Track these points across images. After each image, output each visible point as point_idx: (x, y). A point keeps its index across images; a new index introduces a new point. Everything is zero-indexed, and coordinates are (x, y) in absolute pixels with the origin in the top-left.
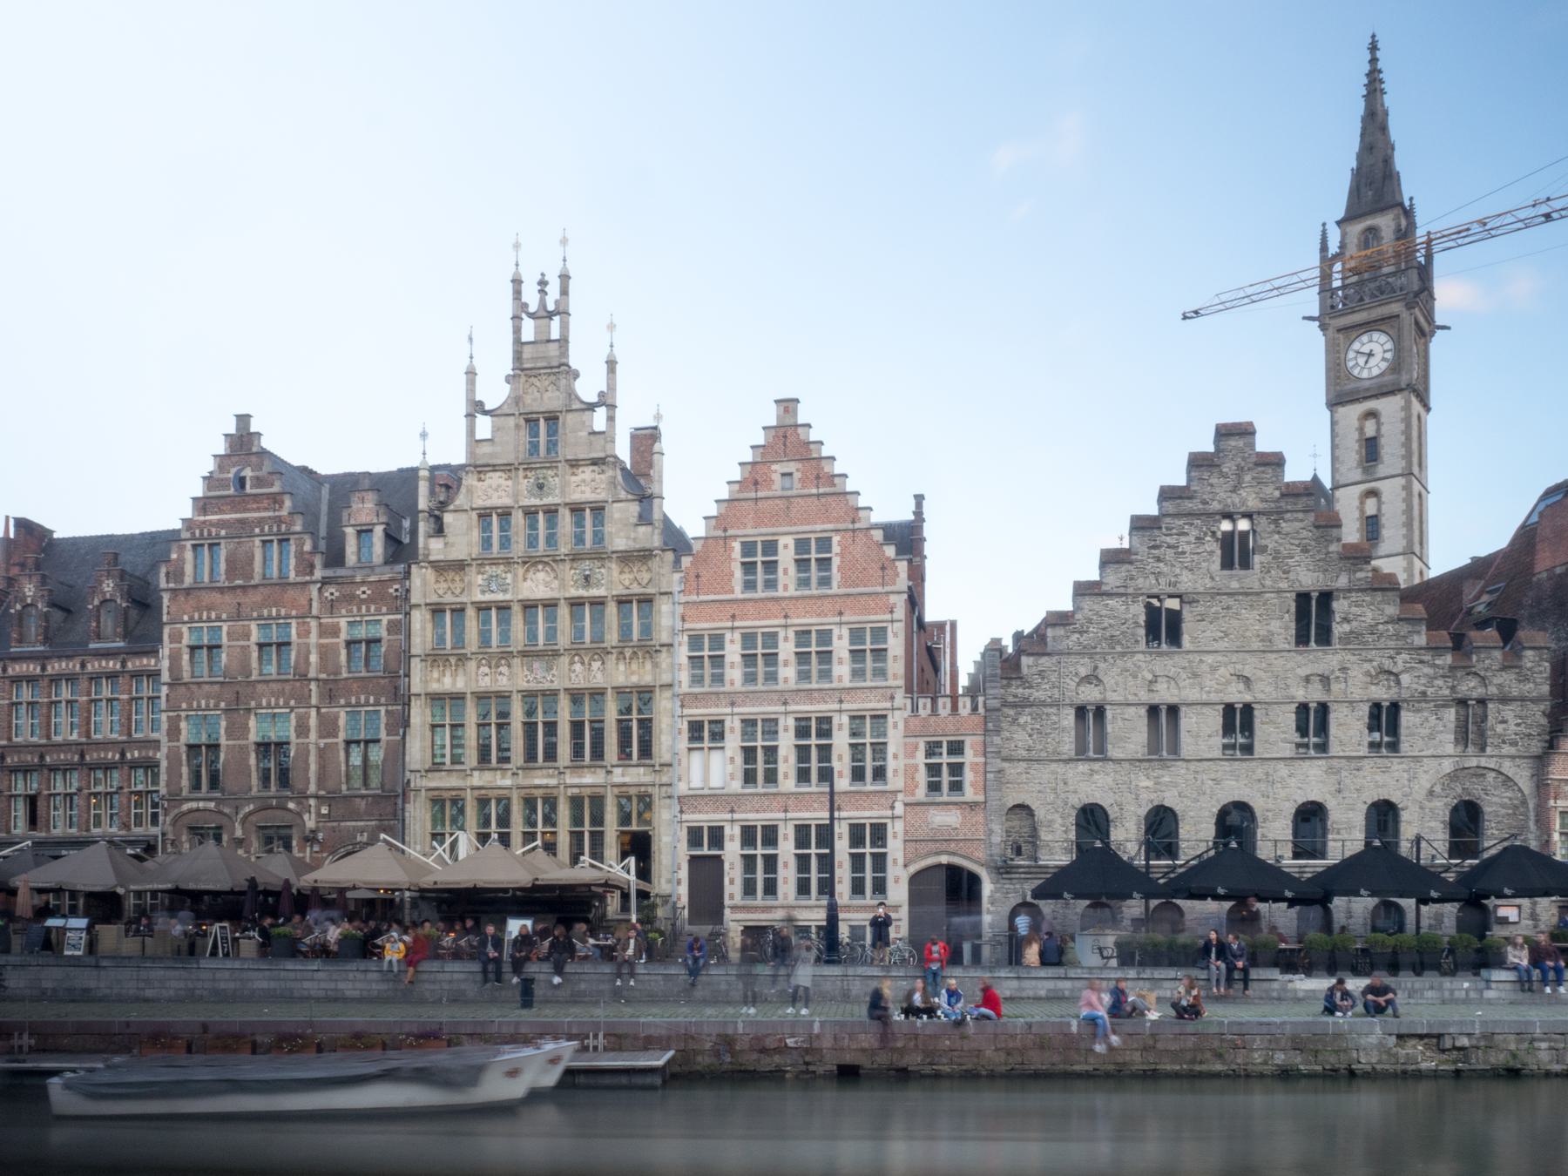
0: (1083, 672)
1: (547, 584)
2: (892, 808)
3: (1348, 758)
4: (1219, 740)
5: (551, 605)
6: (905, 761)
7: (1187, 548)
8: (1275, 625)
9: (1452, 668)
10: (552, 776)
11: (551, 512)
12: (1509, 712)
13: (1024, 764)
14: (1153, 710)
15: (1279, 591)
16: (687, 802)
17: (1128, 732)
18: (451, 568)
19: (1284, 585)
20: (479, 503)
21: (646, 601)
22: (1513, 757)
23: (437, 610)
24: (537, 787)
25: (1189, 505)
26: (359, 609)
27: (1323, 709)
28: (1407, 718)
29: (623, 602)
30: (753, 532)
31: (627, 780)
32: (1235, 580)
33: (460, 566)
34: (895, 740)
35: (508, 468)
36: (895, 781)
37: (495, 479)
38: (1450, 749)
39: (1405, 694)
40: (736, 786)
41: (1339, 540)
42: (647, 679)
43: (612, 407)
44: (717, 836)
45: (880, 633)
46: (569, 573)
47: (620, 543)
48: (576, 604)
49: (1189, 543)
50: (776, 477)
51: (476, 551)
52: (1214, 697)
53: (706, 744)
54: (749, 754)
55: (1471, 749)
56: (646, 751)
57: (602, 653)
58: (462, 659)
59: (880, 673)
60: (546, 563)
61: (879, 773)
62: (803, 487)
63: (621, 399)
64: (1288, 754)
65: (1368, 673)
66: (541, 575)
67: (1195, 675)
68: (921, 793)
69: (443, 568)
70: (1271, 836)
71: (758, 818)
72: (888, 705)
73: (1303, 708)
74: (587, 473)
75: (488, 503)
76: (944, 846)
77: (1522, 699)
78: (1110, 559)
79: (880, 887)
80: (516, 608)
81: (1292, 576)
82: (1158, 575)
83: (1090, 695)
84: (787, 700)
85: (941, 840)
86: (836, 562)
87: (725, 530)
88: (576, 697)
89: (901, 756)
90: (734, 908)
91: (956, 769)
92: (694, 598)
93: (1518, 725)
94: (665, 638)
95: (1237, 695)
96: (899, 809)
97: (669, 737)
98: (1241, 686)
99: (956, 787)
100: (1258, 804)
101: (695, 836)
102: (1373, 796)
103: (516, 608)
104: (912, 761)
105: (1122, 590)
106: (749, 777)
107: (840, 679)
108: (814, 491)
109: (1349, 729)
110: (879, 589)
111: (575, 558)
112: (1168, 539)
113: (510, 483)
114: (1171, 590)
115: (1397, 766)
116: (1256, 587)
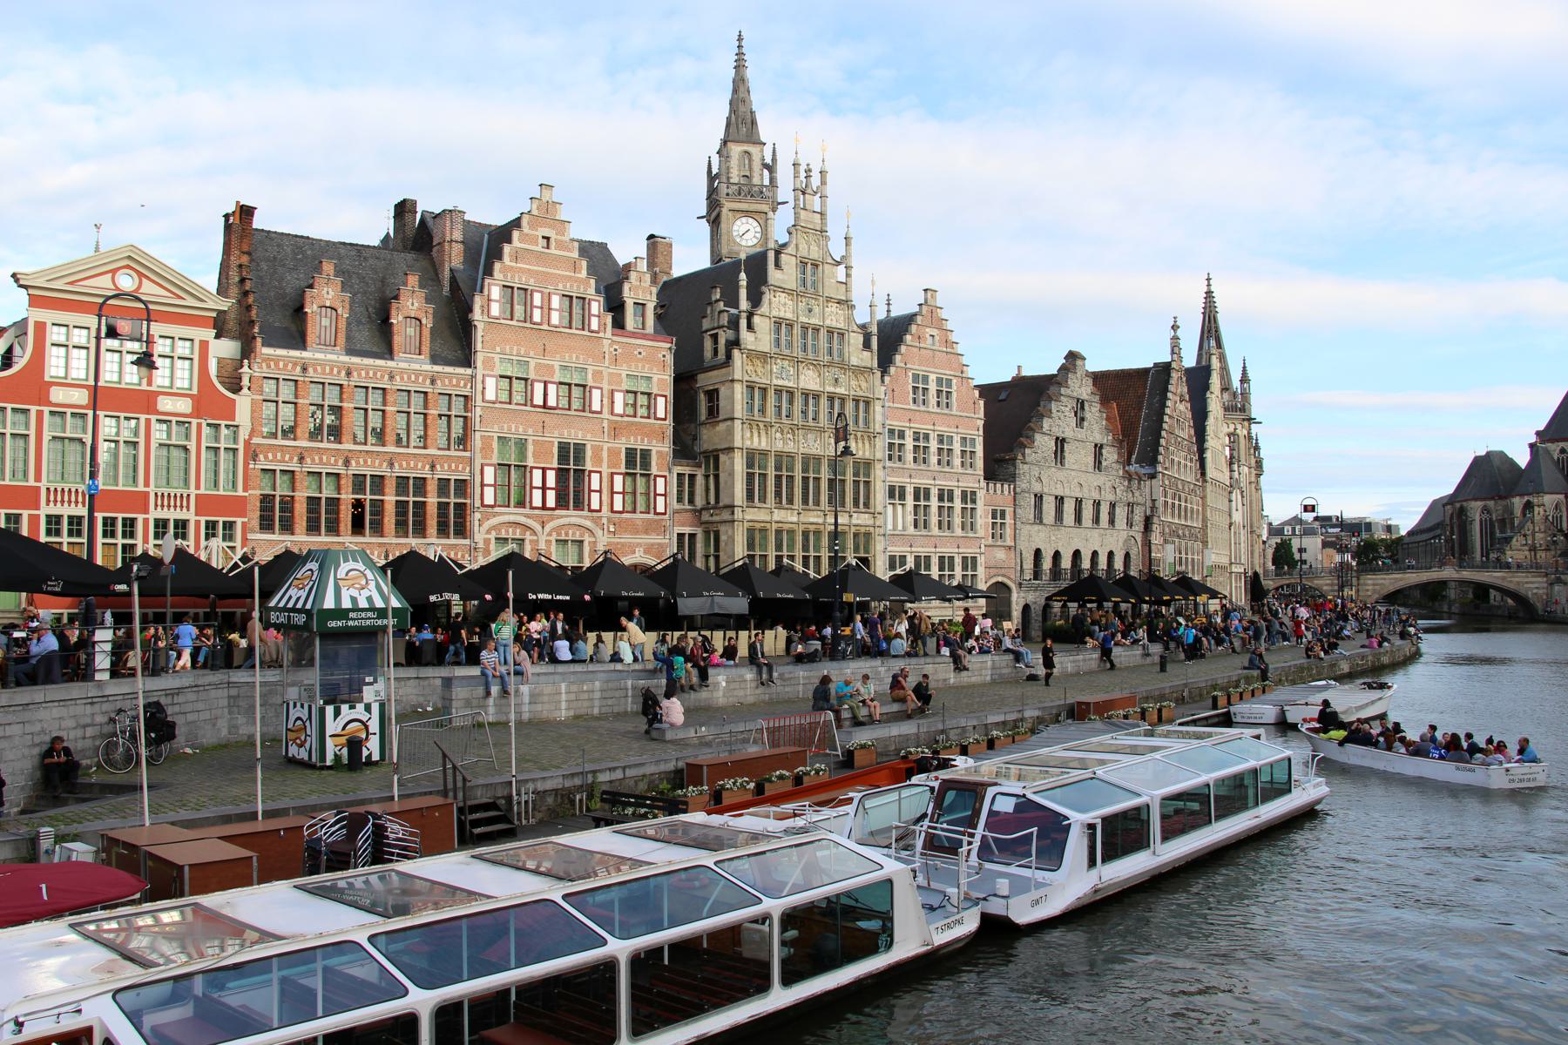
6: (983, 519)
11: (816, 330)
16: (894, 537)
20: (774, 313)
23: (750, 388)
32: (1081, 433)
33: (764, 357)
36: (981, 532)
40: (911, 529)
42: (867, 455)
46: (829, 374)
47: (854, 361)
54: (916, 507)
56: (867, 505)
71: (922, 551)
75: (782, 315)
83: (1037, 488)
84: (931, 478)
86: (954, 395)
94: (878, 428)
95: (1079, 495)
97: (880, 495)
111: (830, 365)
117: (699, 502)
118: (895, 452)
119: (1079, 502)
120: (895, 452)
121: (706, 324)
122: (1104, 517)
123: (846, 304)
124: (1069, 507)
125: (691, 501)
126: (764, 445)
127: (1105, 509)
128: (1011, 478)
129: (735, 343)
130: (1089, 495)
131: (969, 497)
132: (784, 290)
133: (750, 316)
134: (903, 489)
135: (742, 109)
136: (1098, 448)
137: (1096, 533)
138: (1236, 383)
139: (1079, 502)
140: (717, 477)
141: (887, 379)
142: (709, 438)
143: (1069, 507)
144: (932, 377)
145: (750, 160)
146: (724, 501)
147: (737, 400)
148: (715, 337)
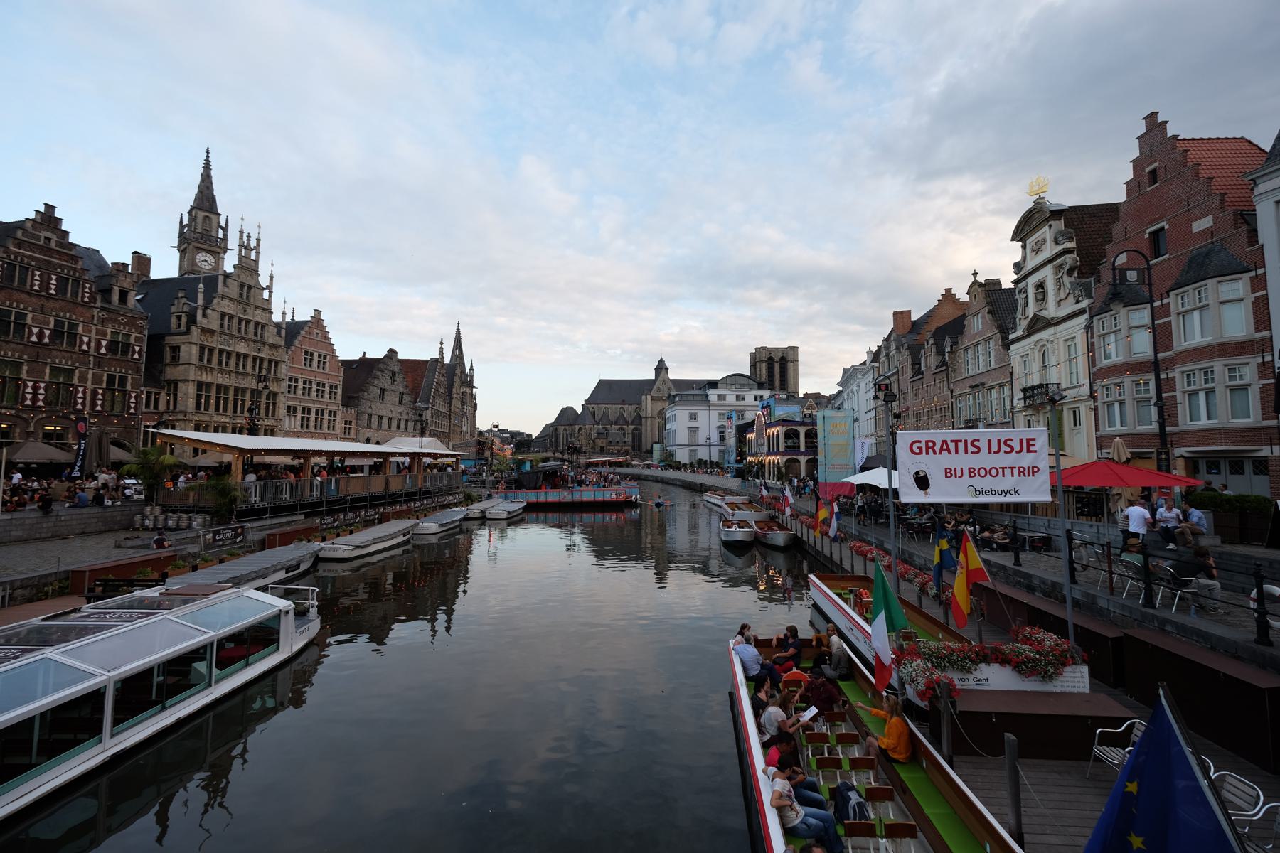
5: (246, 356)
11: (248, 322)
17: (375, 421)
21: (277, 363)
23: (202, 348)
29: (270, 361)
30: (307, 348)
32: (393, 388)
33: (212, 332)
34: (338, 418)
35: (233, 300)
37: (227, 302)
43: (271, 292)
47: (271, 341)
48: (255, 359)
56: (273, 415)
63: (274, 290)
69: (204, 331)
74: (259, 312)
80: (234, 355)
83: (369, 411)
97: (281, 411)
103: (234, 355)
111: (255, 341)
117: (162, 407)
118: (292, 389)
119: (390, 419)
120: (292, 389)
121: (173, 309)
122: (402, 426)
123: (268, 311)
124: (385, 421)
125: (156, 406)
126: (209, 379)
127: (403, 423)
128: (356, 406)
129: (192, 320)
130: (395, 415)
131: (333, 414)
132: (229, 298)
133: (205, 308)
134: (295, 408)
136: (401, 395)
138: (468, 370)
139: (390, 419)
140: (175, 395)
142: (171, 373)
143: (385, 421)
144: (316, 354)
145: (211, 222)
146: (180, 407)
147: (190, 352)
148: (179, 318)
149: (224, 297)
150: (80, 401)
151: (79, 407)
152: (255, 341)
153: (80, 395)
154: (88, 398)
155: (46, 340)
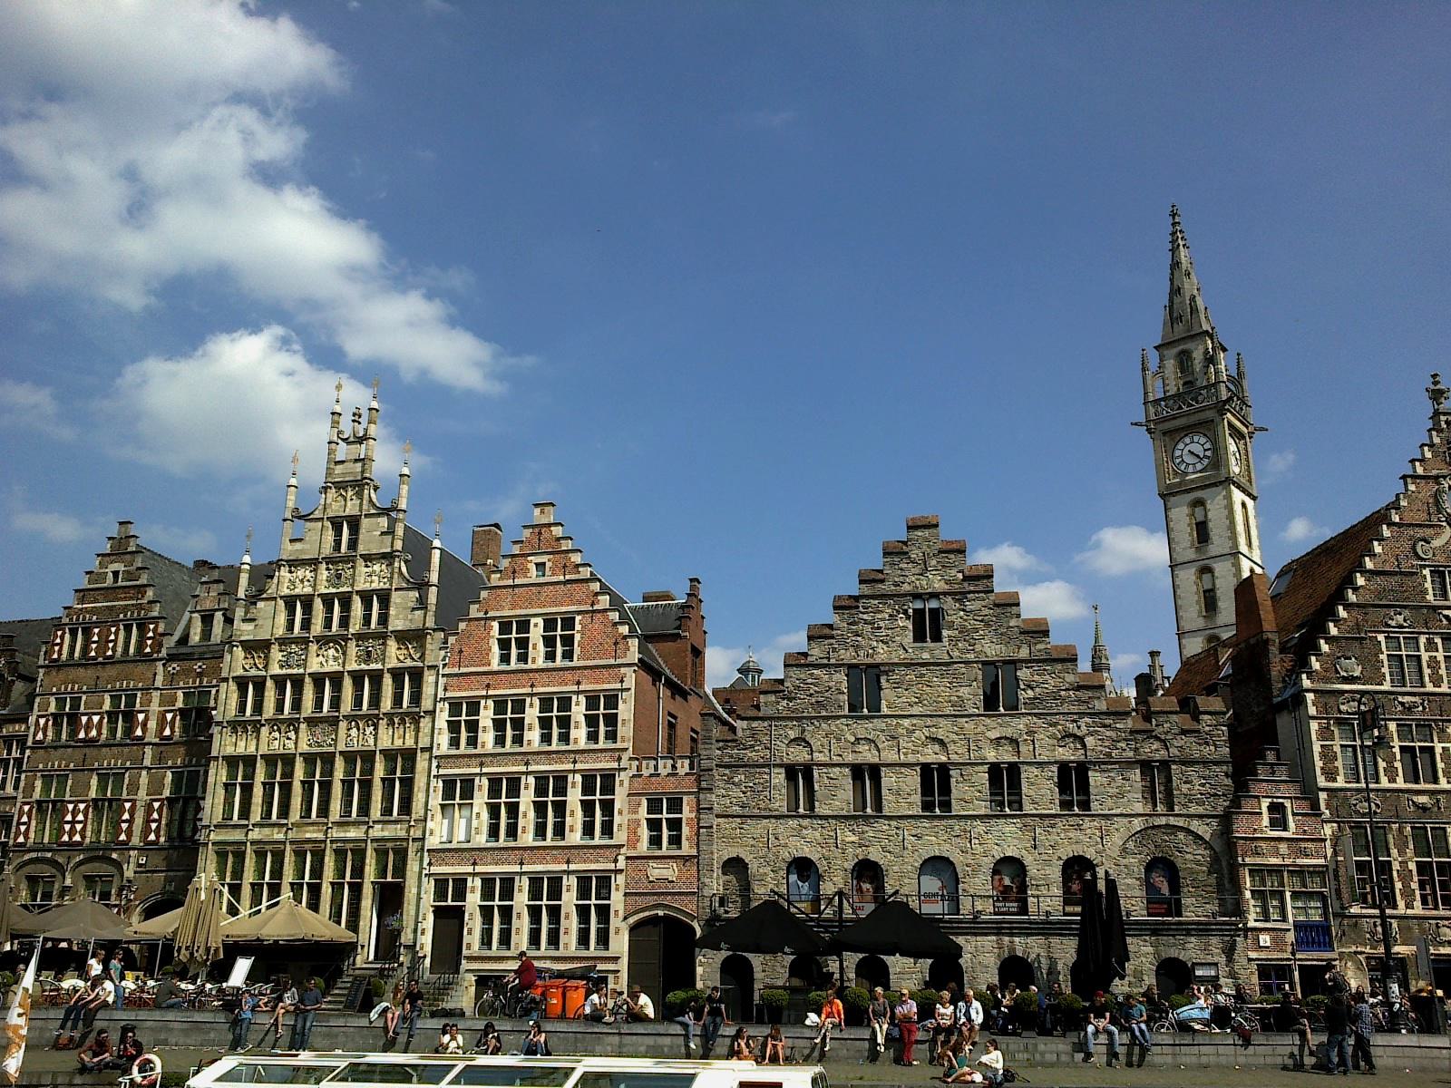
0: (792, 734)
1: (335, 659)
2: (616, 861)
3: (1041, 816)
4: (917, 798)
5: (336, 679)
6: (630, 815)
7: (882, 624)
8: (964, 691)
9: (1132, 732)
10: (319, 831)
12: (1191, 771)
13: (739, 820)
14: (857, 771)
15: (967, 663)
18: (258, 647)
19: (971, 656)
20: (286, 592)
22: (1201, 817)
23: (242, 683)
24: (309, 841)
25: (887, 588)
26: (194, 682)
27: (1014, 769)
28: (1095, 778)
29: (397, 675)
31: (386, 834)
34: (620, 798)
35: (313, 563)
36: (620, 836)
38: (1139, 808)
39: (1091, 756)
40: (481, 839)
41: (1018, 616)
42: (410, 743)
44: (460, 885)
45: (612, 700)
48: (357, 678)
49: (882, 620)
50: (529, 566)
51: (280, 631)
52: (911, 759)
53: (458, 800)
54: (494, 811)
55: (1160, 808)
56: (406, 807)
57: (373, 720)
58: (257, 726)
59: (612, 736)
60: (336, 642)
61: (608, 829)
62: (553, 575)
64: (982, 812)
65: (1052, 736)
66: (332, 652)
67: (893, 738)
68: (643, 847)
69: (252, 647)
70: (972, 891)
72: (615, 765)
73: (995, 770)
76: (661, 900)
77: (1205, 763)
78: (817, 634)
79: (604, 939)
81: (978, 647)
82: (857, 647)
83: (799, 755)
85: (659, 891)
86: (577, 638)
87: (486, 613)
88: (350, 757)
89: (625, 812)
90: (470, 959)
91: (675, 825)
92: (456, 670)
93: (1203, 785)
95: (932, 755)
96: (621, 864)
97: (428, 794)
98: (937, 747)
99: (676, 841)
100: (957, 858)
101: (441, 884)
102: (1067, 852)
104: (634, 817)
105: (825, 661)
106: (494, 832)
107: (576, 741)
108: (562, 578)
109: (1040, 790)
110: (612, 661)
112: (865, 617)
113: (312, 574)
114: (869, 661)
115: (1087, 823)
116: (946, 659)
126: (252, 749)
135: (1177, 300)
137: (1009, 828)
141: (452, 640)
149: (294, 564)
150: (124, 826)
151: (123, 837)
152: (360, 637)
153: (126, 816)
154: (139, 821)
155: (94, 733)
